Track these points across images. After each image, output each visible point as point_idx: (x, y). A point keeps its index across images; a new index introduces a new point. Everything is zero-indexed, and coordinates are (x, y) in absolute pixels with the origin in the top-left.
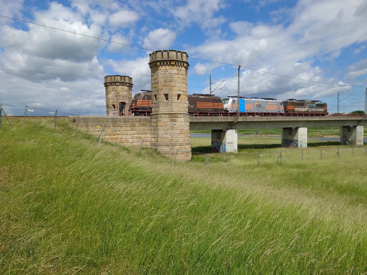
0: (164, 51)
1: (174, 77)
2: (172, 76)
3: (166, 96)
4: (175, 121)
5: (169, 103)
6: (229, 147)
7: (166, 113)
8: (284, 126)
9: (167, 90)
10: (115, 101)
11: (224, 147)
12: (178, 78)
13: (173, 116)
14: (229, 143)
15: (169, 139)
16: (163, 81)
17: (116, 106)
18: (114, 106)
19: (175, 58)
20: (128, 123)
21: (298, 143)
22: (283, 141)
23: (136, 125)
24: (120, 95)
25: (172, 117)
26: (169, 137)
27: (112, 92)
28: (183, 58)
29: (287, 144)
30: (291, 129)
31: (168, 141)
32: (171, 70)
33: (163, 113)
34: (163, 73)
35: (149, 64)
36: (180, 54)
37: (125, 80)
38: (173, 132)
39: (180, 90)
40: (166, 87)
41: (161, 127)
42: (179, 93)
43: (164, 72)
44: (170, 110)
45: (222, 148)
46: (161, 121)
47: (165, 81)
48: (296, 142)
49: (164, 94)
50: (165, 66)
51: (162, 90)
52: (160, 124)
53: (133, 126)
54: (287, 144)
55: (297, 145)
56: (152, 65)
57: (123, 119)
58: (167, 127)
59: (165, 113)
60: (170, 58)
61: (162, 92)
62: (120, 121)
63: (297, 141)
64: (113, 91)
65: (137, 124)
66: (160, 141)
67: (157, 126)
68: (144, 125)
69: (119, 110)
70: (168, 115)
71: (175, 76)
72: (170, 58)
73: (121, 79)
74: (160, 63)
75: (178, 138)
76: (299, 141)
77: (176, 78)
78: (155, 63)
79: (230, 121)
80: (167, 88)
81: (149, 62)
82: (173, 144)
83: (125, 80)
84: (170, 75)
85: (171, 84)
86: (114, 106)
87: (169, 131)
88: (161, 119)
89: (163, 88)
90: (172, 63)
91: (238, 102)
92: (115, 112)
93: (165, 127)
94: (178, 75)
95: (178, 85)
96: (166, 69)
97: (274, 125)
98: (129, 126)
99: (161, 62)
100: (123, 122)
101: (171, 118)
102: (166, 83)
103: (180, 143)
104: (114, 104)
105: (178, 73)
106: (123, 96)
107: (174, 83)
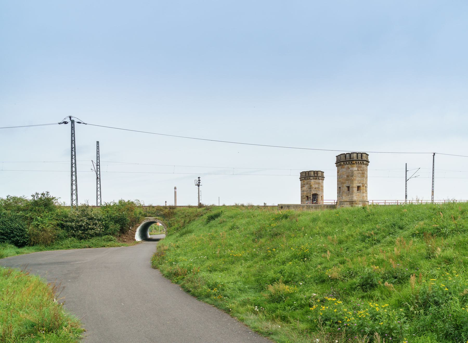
0: (347, 154)
1: (354, 173)
2: (353, 172)
3: (348, 187)
7: (348, 201)
10: (309, 193)
12: (358, 174)
16: (346, 177)
17: (309, 197)
18: (307, 197)
19: (355, 158)
24: (313, 188)
27: (306, 186)
28: (363, 157)
32: (352, 168)
33: (345, 201)
34: (346, 170)
35: (335, 163)
36: (360, 154)
37: (317, 174)
39: (360, 183)
42: (359, 185)
43: (347, 169)
47: (348, 176)
49: (347, 186)
50: (348, 165)
56: (337, 164)
57: (315, 206)
60: (352, 158)
61: (345, 185)
64: (307, 184)
69: (311, 201)
70: (349, 202)
71: (355, 172)
72: (352, 158)
73: (314, 174)
74: (344, 163)
77: (356, 174)
78: (340, 163)
81: (336, 162)
83: (317, 174)
84: (352, 172)
86: (307, 197)
89: (345, 182)
90: (353, 163)
92: (308, 202)
94: (358, 171)
95: (357, 179)
99: (345, 162)
100: (315, 208)
104: (307, 195)
105: (358, 169)
106: (315, 188)
107: (354, 177)
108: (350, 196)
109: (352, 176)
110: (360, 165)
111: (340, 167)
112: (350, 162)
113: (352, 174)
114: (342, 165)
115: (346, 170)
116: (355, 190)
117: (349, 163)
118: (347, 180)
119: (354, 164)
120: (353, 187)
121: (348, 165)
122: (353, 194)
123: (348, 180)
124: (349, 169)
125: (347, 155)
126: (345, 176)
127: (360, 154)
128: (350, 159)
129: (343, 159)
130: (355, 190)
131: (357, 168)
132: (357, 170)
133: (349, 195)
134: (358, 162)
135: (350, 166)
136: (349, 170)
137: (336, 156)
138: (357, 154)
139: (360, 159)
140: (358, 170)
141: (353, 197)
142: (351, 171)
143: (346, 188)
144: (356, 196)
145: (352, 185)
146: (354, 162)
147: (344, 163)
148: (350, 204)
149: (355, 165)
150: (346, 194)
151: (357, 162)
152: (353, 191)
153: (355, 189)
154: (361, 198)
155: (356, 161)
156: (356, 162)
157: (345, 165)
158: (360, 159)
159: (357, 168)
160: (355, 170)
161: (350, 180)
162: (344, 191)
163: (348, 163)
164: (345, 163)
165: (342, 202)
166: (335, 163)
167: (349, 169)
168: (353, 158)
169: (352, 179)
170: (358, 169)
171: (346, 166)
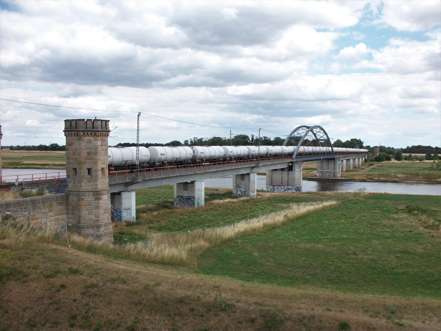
1: (99, 149)
3: (89, 170)
4: (100, 199)
5: (92, 179)
6: (126, 214)
8: (181, 181)
9: (91, 164)
11: (119, 214)
12: (102, 150)
13: (97, 194)
14: (126, 209)
15: (94, 220)
16: (86, 154)
20: (46, 204)
21: (194, 200)
22: (177, 197)
23: (54, 205)
25: (98, 195)
26: (94, 217)
29: (182, 202)
30: (187, 183)
31: (92, 223)
32: (95, 142)
33: (87, 190)
38: (98, 212)
39: (104, 164)
40: (89, 161)
41: (83, 206)
44: (94, 186)
45: (117, 216)
46: (85, 200)
47: (89, 154)
48: (192, 199)
50: (89, 136)
51: (85, 163)
52: (83, 203)
53: (51, 205)
54: (182, 202)
55: (194, 203)
57: (42, 200)
58: (91, 206)
59: (89, 191)
60: (96, 128)
61: (85, 166)
62: (39, 203)
63: (194, 198)
65: (54, 203)
66: (83, 222)
67: (80, 206)
68: (61, 204)
72: (96, 128)
74: (84, 133)
75: (102, 218)
76: (196, 198)
79: (128, 181)
80: (90, 162)
82: (99, 225)
85: (96, 157)
87: (93, 211)
88: (84, 197)
89: (85, 162)
90: (97, 134)
91: (137, 157)
93: (89, 206)
94: (102, 146)
96: (89, 140)
97: (171, 181)
98: (48, 207)
100: (42, 203)
101: (95, 196)
102: (89, 156)
103: (105, 224)
105: (102, 144)
108: (92, 183)
109: (96, 154)
110: (104, 137)
111: (73, 139)
112: (93, 133)
113: (95, 150)
114: (80, 135)
115: (86, 144)
116: (99, 174)
117: (91, 134)
118: (87, 159)
119: (98, 136)
120: (97, 171)
121: (89, 138)
122: (97, 180)
123: (89, 159)
124: (91, 143)
125: (89, 122)
126: (85, 153)
127: (104, 122)
128: (93, 128)
129: (83, 127)
130: (99, 174)
131: (101, 142)
132: (101, 145)
133: (91, 182)
134: (103, 134)
135: (92, 138)
136: (91, 144)
137: (65, 121)
138: (102, 121)
139: (104, 129)
140: (102, 145)
141: (97, 185)
142: (94, 147)
143: (87, 171)
144: (101, 183)
145: (96, 167)
146: (98, 134)
147: (84, 133)
148: (94, 196)
149: (99, 138)
150: (87, 180)
151: (102, 133)
152: (97, 176)
153: (100, 173)
154: (106, 185)
155: (100, 133)
156: (101, 134)
157: (85, 136)
158: (104, 129)
159: (101, 142)
160: (99, 146)
161: (93, 160)
162: (84, 176)
163: (89, 133)
164: (86, 133)
165: (83, 192)
166: (63, 131)
167: (91, 143)
168: (98, 128)
169: (95, 158)
170: (102, 143)
171: (86, 138)
